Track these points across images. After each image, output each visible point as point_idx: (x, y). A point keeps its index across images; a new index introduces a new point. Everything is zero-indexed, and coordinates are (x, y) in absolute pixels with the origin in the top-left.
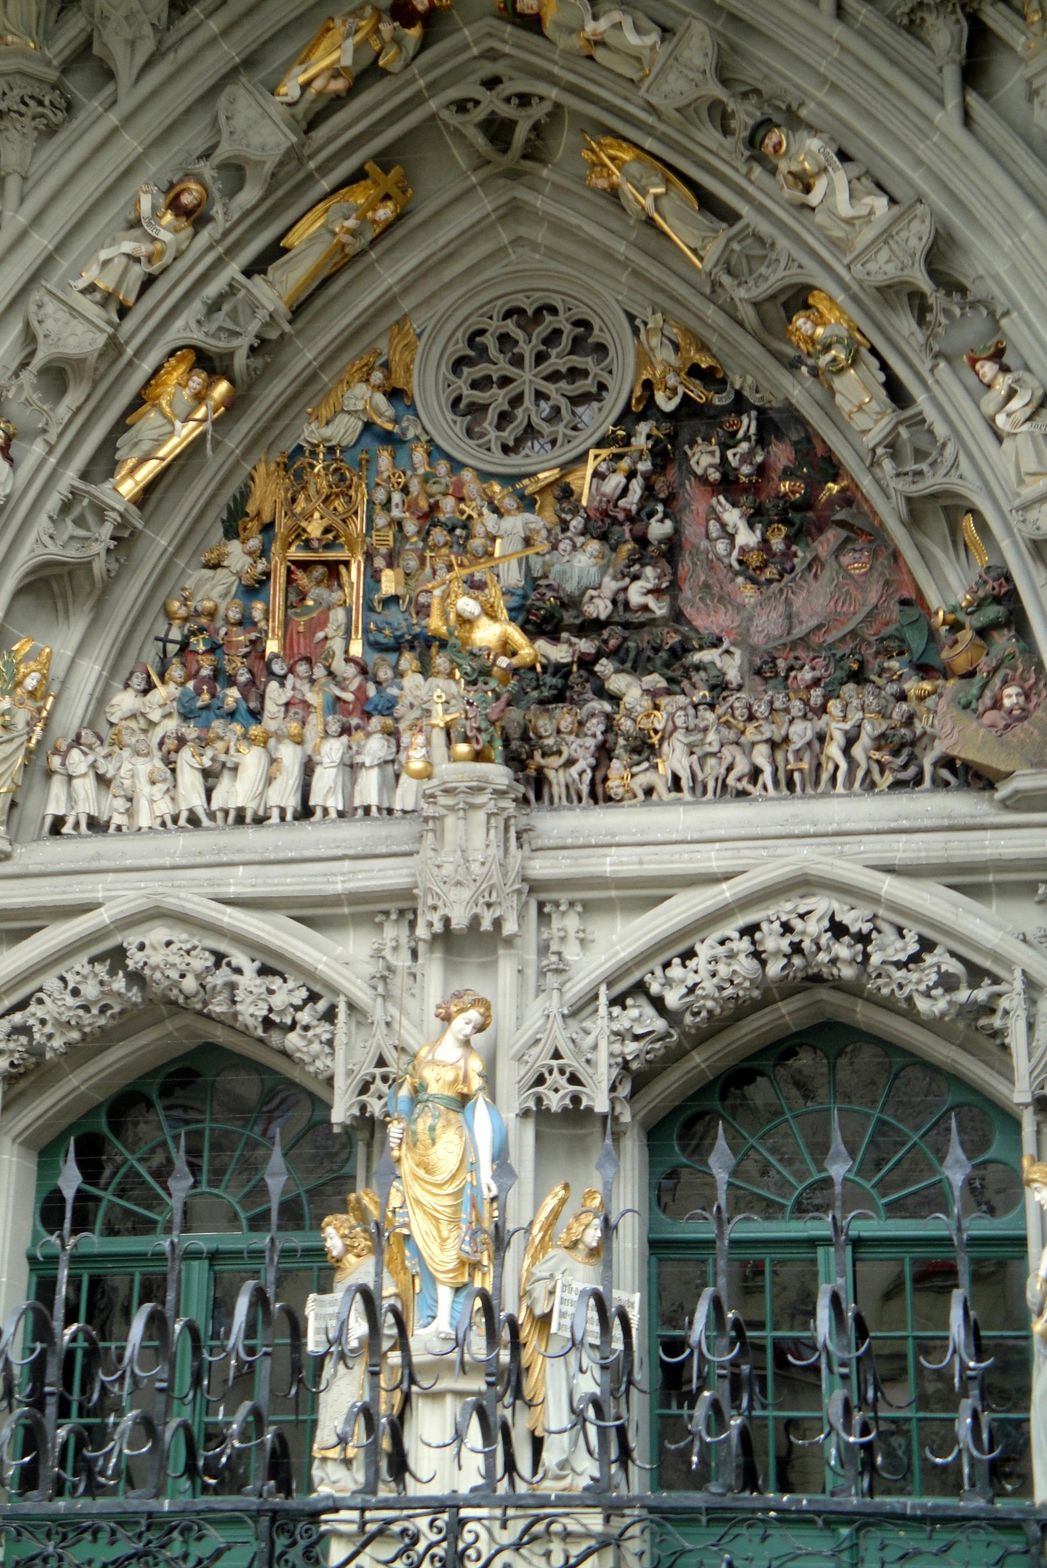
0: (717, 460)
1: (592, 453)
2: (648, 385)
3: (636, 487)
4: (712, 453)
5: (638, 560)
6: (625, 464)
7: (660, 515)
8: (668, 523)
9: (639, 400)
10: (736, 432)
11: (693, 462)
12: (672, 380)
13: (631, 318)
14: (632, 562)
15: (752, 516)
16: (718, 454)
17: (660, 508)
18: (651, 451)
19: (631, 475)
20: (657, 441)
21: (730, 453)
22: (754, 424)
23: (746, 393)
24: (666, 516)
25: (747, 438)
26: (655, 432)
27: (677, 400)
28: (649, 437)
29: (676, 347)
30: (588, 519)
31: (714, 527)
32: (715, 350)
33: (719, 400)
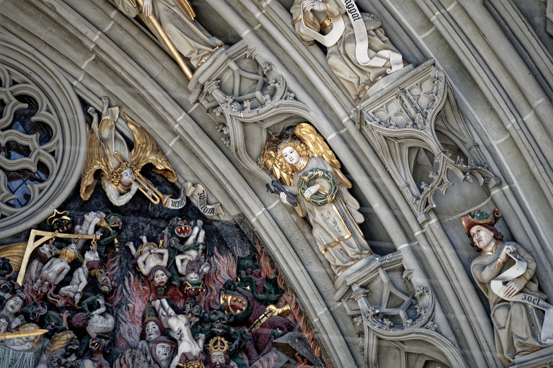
0: (164, 263)
1: (34, 233)
2: (98, 174)
3: (81, 275)
4: (161, 255)
5: (72, 351)
6: (71, 251)
7: (103, 309)
8: (111, 320)
9: (88, 187)
10: (186, 239)
11: (140, 261)
12: (127, 176)
13: (85, 105)
14: (68, 352)
15: (196, 324)
16: (166, 257)
17: (101, 301)
18: (98, 242)
19: (75, 264)
20: (106, 233)
21: (178, 259)
22: (203, 233)
23: (196, 201)
24: (109, 311)
25: (195, 246)
26: (104, 224)
27: (128, 197)
28: (97, 228)
29: (131, 145)
30: (25, 302)
31: (152, 327)
32: (169, 153)
33: (170, 204)
